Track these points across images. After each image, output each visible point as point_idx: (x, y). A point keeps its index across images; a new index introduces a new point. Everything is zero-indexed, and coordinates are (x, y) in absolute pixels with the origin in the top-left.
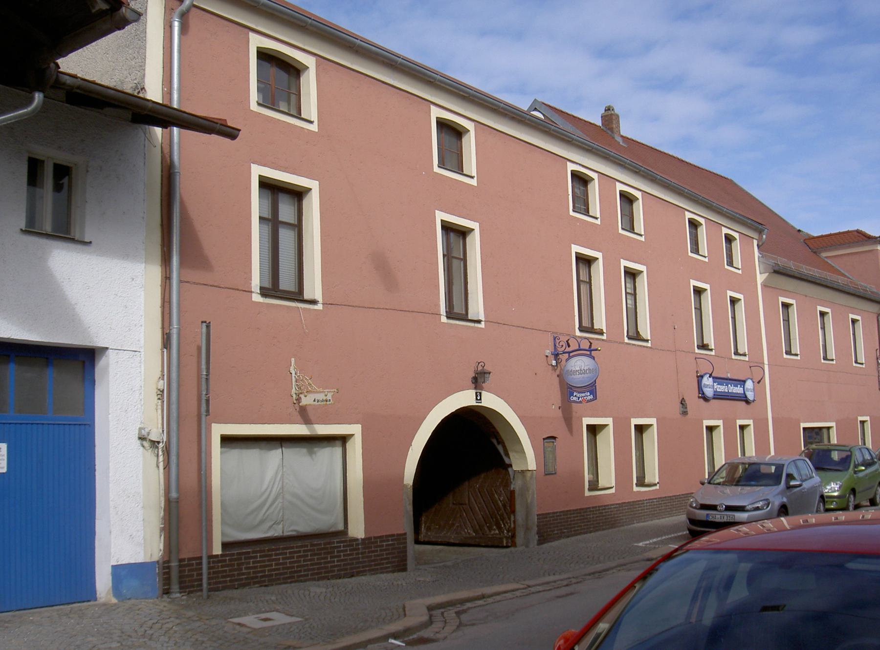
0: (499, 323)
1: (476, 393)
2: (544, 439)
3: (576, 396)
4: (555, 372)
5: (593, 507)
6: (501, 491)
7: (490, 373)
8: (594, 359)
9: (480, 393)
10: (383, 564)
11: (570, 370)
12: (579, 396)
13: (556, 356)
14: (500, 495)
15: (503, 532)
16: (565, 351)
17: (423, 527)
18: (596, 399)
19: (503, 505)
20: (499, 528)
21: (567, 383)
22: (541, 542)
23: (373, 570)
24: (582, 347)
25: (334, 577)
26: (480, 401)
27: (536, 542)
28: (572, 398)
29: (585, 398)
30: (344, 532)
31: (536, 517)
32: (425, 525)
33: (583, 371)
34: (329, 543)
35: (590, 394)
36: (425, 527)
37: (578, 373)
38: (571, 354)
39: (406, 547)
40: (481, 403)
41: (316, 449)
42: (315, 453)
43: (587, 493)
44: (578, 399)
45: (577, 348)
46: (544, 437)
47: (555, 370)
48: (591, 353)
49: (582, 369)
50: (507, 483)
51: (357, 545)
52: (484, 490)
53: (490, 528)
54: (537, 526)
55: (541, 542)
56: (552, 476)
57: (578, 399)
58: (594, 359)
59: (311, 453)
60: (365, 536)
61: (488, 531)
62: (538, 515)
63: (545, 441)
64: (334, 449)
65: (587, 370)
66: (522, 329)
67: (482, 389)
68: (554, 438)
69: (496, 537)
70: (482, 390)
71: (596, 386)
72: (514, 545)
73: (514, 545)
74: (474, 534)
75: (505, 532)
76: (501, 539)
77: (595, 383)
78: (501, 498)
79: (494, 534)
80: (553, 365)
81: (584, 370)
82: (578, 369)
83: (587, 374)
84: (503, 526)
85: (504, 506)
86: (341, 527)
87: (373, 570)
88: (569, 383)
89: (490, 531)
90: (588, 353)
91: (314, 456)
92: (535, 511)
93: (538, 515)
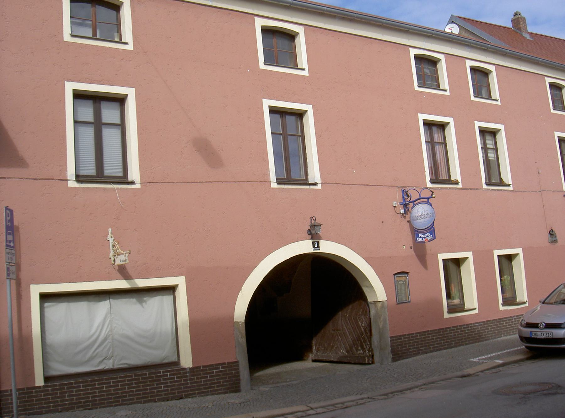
0: (337, 184)
1: (313, 243)
2: (394, 275)
3: (420, 237)
4: (405, 218)
5: (453, 327)
6: (362, 319)
7: (321, 225)
9: (318, 243)
10: (214, 387)
11: (415, 216)
12: (422, 237)
13: (405, 206)
14: (362, 323)
15: (366, 352)
16: (411, 200)
18: (435, 238)
19: (364, 330)
20: (363, 348)
21: (414, 227)
22: (394, 360)
23: (203, 392)
24: (422, 196)
25: (160, 400)
26: (318, 249)
27: (390, 360)
28: (418, 239)
30: (177, 363)
32: (316, 346)
33: (424, 216)
34: (155, 373)
35: (430, 235)
36: (315, 348)
37: (420, 218)
38: (415, 203)
39: (238, 372)
40: (319, 250)
41: (145, 299)
42: (145, 301)
43: (446, 315)
44: (423, 240)
45: (419, 197)
46: (395, 273)
47: (405, 217)
48: (428, 201)
49: (423, 214)
50: (366, 312)
51: (186, 373)
52: (351, 318)
53: (357, 350)
54: (391, 346)
55: (394, 360)
56: (409, 304)
57: (423, 240)
59: (141, 302)
60: (193, 366)
61: (355, 352)
62: (391, 337)
63: (395, 276)
65: (426, 214)
67: (320, 238)
68: (407, 273)
69: (360, 356)
70: (320, 239)
71: (434, 227)
72: (373, 363)
73: (373, 363)
74: (347, 354)
75: (367, 352)
76: (364, 357)
77: (434, 225)
79: (359, 354)
80: (401, 213)
81: (424, 215)
82: (420, 214)
83: (427, 218)
84: (365, 347)
85: (365, 330)
87: (203, 392)
88: (415, 227)
89: (357, 351)
90: (426, 200)
91: (144, 304)
92: (388, 335)
93: (391, 337)
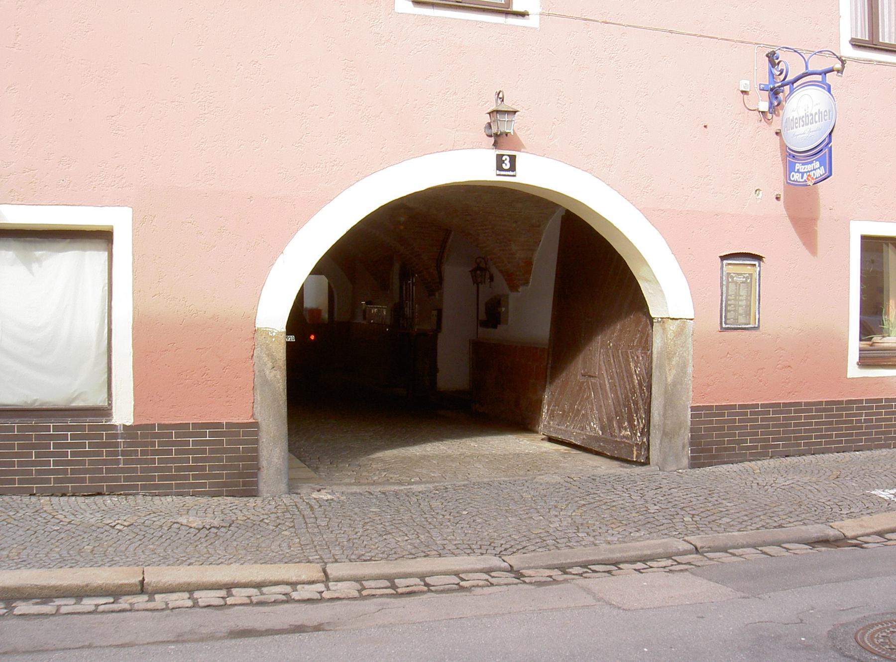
0: (586, 20)
1: (499, 158)
2: (723, 258)
3: (798, 171)
4: (770, 124)
5: (868, 401)
6: (638, 357)
7: (515, 112)
8: (829, 92)
9: (513, 159)
10: (186, 477)
11: (791, 118)
12: (802, 171)
13: (774, 92)
14: (636, 366)
15: (636, 434)
16: (786, 80)
17: (545, 410)
18: (830, 174)
19: (638, 383)
20: (632, 427)
21: (787, 146)
22: (695, 463)
23: (156, 487)
24: (811, 69)
25: (43, 492)
26: (511, 173)
27: (685, 461)
28: (793, 176)
29: (811, 174)
30: (104, 412)
31: (689, 413)
32: (549, 406)
33: (810, 118)
34: (33, 428)
35: (821, 166)
36: (548, 410)
37: (802, 123)
38: (795, 85)
39: (256, 450)
40: (514, 176)
41: (38, 253)
42: (39, 260)
43: (854, 371)
44: (802, 178)
45: (804, 71)
46: (722, 254)
47: (769, 121)
48: (824, 79)
49: (809, 114)
50: (646, 344)
51: (116, 436)
52: (618, 352)
53: (621, 427)
54: (692, 430)
55: (695, 463)
56: (754, 332)
57: (802, 178)
58: (829, 92)
59: (27, 263)
60: (134, 423)
61: (617, 431)
62: (693, 408)
63: (725, 262)
64: (7, 252)
65: (816, 113)
66: (608, 21)
67: (519, 146)
68: (759, 258)
69: (624, 442)
70: (519, 151)
71: (831, 147)
72: (647, 463)
73: (647, 463)
74: (600, 433)
75: (639, 434)
76: (631, 446)
77: (830, 141)
78: (637, 370)
79: (624, 437)
80: (761, 110)
81: (811, 115)
82: (802, 114)
83: (816, 122)
84: (636, 423)
85: (640, 384)
86: (99, 400)
87: (156, 487)
88: (788, 145)
89: (620, 431)
90: (819, 78)
91: (35, 266)
92: (688, 400)
93: (693, 408)
